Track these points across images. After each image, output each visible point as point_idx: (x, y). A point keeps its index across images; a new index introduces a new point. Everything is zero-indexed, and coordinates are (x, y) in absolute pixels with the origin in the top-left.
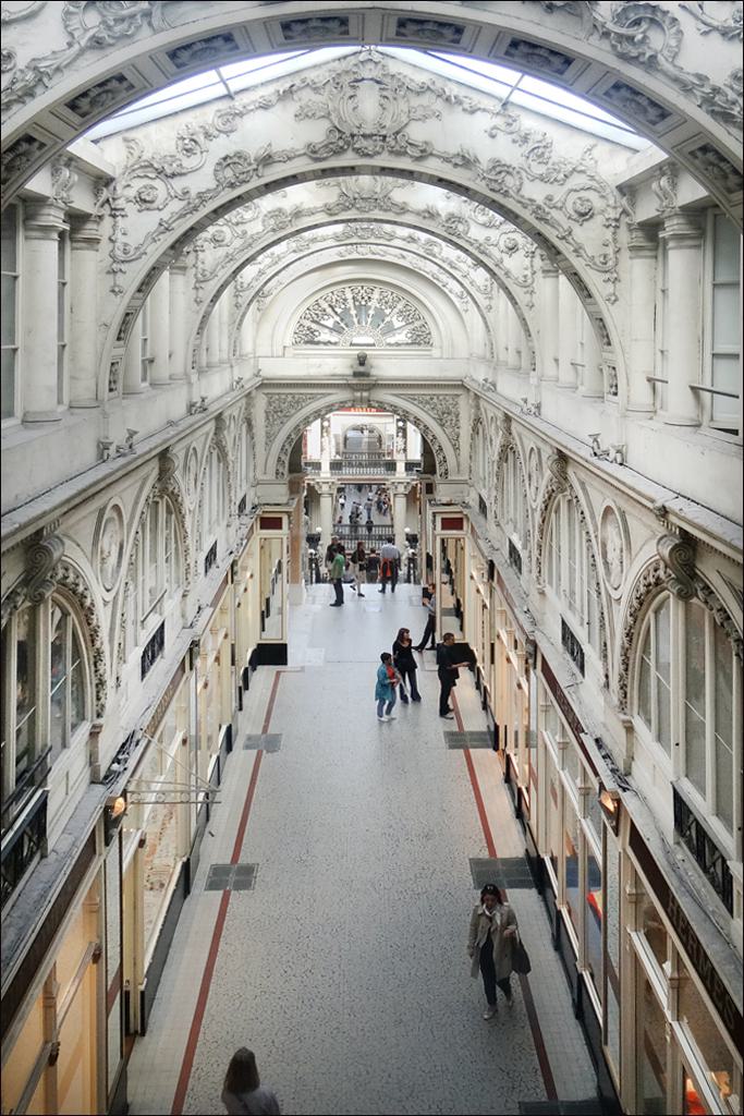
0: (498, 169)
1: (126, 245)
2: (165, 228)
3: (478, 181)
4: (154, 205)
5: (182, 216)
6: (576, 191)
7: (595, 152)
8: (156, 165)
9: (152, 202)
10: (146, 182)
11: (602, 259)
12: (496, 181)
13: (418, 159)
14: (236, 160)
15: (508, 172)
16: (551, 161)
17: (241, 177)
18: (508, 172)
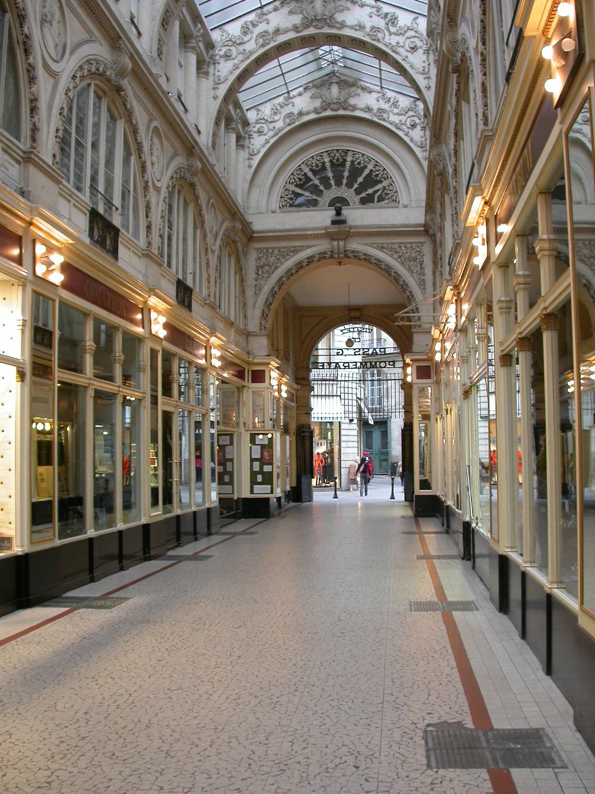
0: (374, 30)
1: (219, 76)
2: (236, 67)
3: (366, 36)
4: (232, 58)
5: (243, 61)
6: (409, 38)
7: (418, 21)
8: (233, 40)
9: (230, 56)
10: (228, 48)
11: (422, 68)
12: (373, 35)
13: (340, 29)
14: (264, 34)
15: (379, 31)
16: (398, 26)
17: (267, 42)
18: (379, 31)
